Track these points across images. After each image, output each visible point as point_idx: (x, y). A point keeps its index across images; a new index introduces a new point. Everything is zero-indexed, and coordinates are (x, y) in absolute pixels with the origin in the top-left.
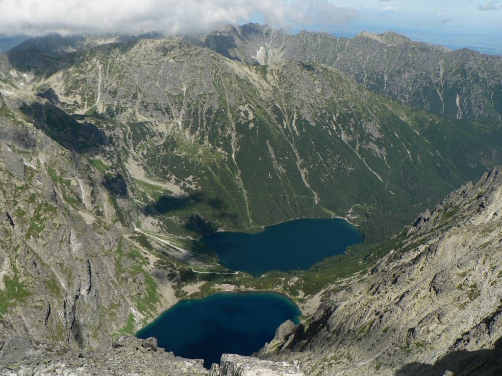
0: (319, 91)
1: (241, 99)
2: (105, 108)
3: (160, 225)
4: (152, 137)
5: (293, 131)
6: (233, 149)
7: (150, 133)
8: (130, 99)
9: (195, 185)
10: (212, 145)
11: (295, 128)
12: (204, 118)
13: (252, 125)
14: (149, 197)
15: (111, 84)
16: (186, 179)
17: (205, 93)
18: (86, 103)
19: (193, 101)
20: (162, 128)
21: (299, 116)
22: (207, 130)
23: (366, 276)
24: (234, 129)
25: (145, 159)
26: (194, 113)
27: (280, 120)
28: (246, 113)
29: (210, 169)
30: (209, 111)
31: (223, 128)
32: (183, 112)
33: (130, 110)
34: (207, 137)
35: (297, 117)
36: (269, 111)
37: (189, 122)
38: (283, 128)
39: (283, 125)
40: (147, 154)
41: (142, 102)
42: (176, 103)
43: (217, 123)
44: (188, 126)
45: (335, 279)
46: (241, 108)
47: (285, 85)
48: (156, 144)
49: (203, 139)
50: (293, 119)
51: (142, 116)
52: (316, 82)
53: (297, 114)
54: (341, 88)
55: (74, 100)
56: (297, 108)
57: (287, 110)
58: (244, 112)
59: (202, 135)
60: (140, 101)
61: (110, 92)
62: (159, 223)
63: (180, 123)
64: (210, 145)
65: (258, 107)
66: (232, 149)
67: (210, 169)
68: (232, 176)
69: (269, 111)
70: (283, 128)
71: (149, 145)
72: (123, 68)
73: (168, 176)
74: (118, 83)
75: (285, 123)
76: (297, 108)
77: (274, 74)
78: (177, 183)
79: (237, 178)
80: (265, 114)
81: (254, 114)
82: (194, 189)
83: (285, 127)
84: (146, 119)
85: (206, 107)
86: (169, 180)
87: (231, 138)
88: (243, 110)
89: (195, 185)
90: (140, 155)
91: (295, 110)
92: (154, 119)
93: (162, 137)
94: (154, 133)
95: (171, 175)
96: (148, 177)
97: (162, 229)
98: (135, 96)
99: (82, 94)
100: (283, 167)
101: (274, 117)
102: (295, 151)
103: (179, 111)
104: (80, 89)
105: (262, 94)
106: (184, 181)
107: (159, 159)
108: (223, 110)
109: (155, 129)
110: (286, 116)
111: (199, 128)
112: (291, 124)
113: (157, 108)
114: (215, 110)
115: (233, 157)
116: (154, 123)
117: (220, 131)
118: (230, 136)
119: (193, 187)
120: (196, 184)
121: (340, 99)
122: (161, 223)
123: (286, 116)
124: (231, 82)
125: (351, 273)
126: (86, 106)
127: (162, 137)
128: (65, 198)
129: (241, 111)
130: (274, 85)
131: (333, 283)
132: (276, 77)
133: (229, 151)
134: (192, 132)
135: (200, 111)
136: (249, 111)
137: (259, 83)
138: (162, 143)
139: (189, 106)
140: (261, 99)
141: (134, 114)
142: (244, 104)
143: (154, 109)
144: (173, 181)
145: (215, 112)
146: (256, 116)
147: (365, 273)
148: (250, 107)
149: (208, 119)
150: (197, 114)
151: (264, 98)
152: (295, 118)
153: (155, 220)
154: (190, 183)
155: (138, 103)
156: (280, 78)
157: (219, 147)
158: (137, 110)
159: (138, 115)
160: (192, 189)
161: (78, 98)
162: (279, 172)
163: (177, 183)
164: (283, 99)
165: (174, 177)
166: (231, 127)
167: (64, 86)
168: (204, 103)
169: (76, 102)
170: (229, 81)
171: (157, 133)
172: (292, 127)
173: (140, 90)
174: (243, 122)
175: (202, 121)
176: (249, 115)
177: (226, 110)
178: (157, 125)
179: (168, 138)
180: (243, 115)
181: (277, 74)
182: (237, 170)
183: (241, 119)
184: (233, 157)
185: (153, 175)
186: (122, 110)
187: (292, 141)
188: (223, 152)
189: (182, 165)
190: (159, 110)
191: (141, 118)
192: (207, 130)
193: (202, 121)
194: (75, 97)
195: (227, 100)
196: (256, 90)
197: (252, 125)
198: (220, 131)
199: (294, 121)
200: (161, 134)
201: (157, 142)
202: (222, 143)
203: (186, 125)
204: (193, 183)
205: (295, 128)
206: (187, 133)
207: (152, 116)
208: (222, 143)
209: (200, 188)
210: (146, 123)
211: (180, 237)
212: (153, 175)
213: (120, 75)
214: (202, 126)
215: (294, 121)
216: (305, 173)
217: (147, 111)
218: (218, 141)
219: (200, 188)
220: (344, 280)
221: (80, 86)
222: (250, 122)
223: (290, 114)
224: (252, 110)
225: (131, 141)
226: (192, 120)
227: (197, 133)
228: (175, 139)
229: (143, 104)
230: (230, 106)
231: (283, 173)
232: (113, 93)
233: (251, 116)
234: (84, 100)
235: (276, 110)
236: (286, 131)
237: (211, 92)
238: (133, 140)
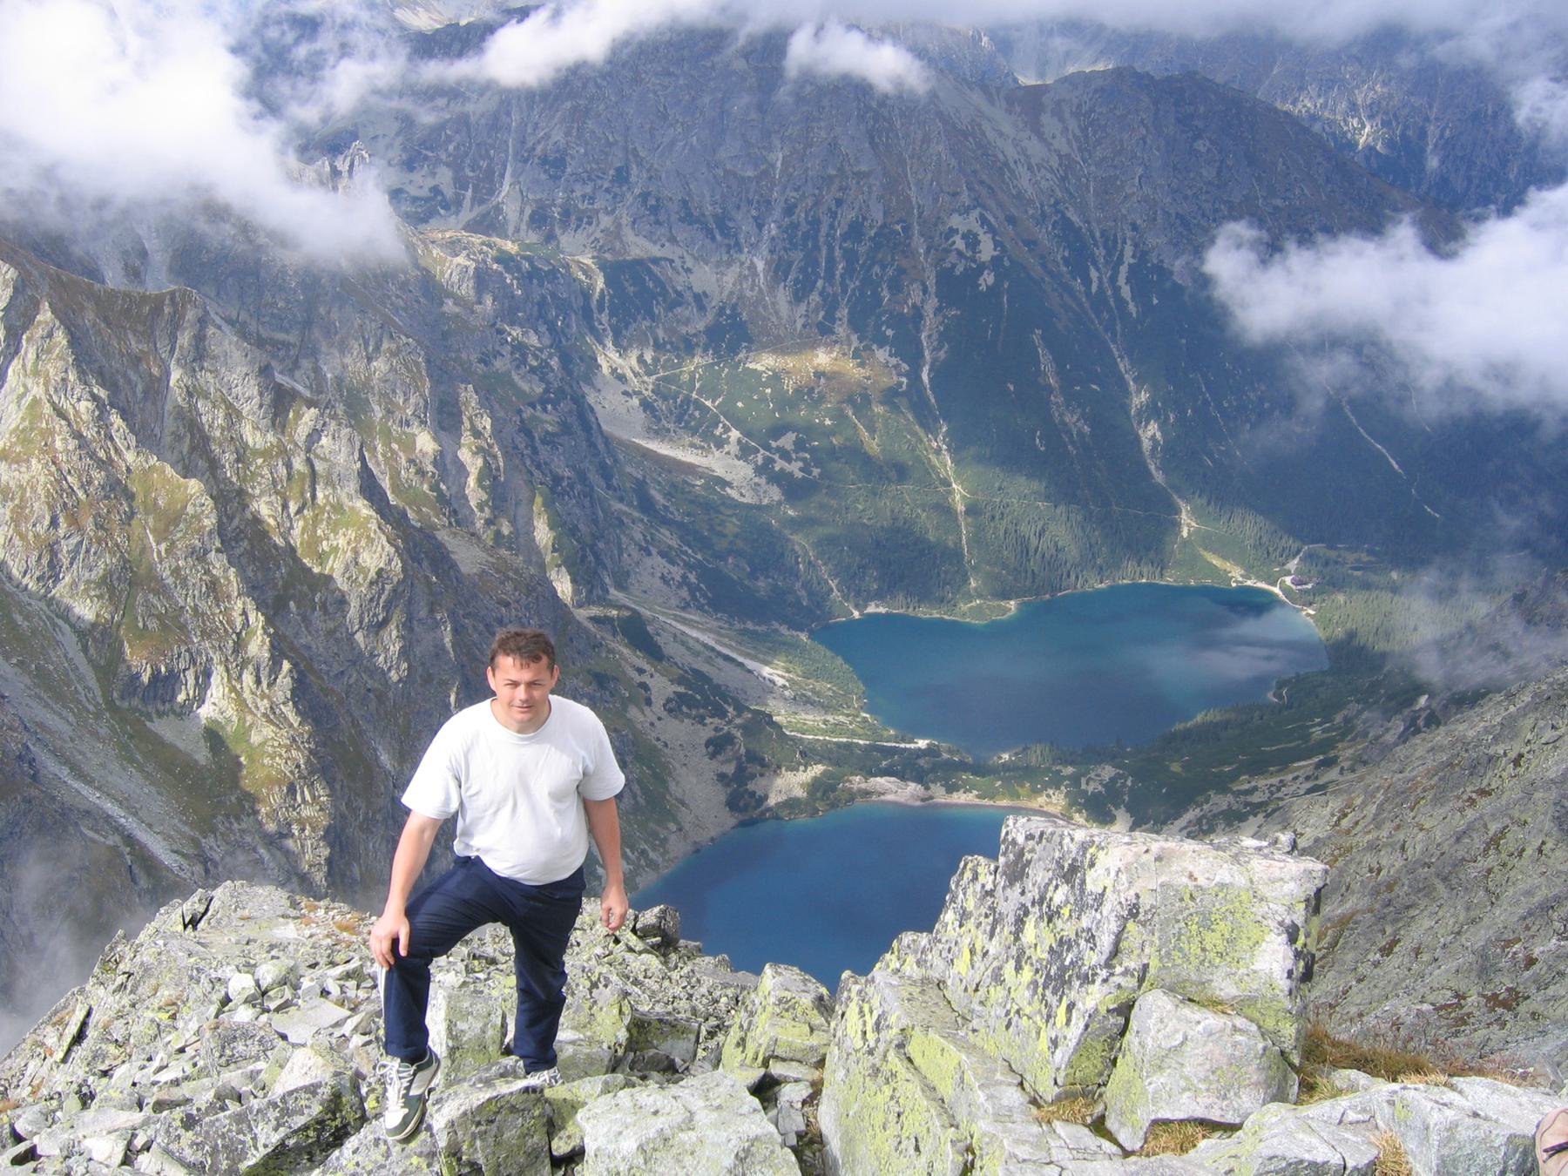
0: (1208, 173)
1: (955, 194)
2: (528, 211)
3: (689, 585)
4: (671, 307)
5: (1121, 302)
6: (927, 353)
7: (665, 293)
8: (606, 185)
9: (800, 464)
10: (860, 339)
11: (1126, 292)
12: (838, 253)
13: (987, 279)
14: (658, 497)
15: (547, 136)
16: (774, 444)
17: (841, 170)
18: (469, 193)
19: (803, 197)
20: (704, 278)
21: (1142, 255)
22: (844, 291)
23: (1333, 774)
24: (932, 289)
25: (649, 374)
26: (806, 236)
27: (1080, 260)
28: (972, 241)
30: (855, 231)
31: (896, 287)
32: (772, 229)
33: (606, 221)
34: (843, 313)
36: (1043, 235)
37: (790, 264)
38: (1088, 293)
39: (1087, 282)
40: (656, 360)
41: (645, 196)
42: (750, 202)
43: (877, 269)
44: (786, 276)
45: (1234, 777)
46: (956, 221)
47: (1098, 154)
48: (683, 330)
49: (830, 317)
50: (1120, 261)
51: (642, 241)
52: (1201, 146)
53: (1136, 246)
54: (1280, 166)
55: (430, 183)
56: (1135, 227)
57: (1103, 233)
58: (963, 237)
59: (830, 306)
60: (637, 191)
61: (544, 160)
62: (684, 577)
63: (760, 265)
64: (854, 337)
65: (1011, 220)
66: (921, 354)
68: (922, 441)
69: (1043, 235)
70: (1088, 293)
71: (661, 333)
72: (584, 86)
73: (717, 432)
74: (568, 134)
75: (1094, 274)
76: (1135, 227)
77: (1067, 115)
78: (745, 453)
80: (1031, 243)
81: (996, 244)
82: (799, 475)
84: (655, 251)
85: (848, 215)
86: (720, 443)
87: (921, 317)
88: (963, 229)
89: (800, 464)
90: (634, 361)
91: (1129, 234)
92: (679, 251)
93: (702, 308)
94: (679, 294)
95: (727, 430)
96: (657, 432)
97: (694, 598)
98: (622, 177)
99: (456, 166)
100: (1083, 415)
101: (1061, 253)
103: (760, 227)
104: (451, 148)
105: (1025, 182)
106: (768, 448)
107: (692, 379)
108: (898, 227)
109: (680, 281)
110: (1100, 252)
111: (820, 283)
112: (1113, 279)
113: (689, 216)
114: (871, 227)
115: (925, 377)
116: (678, 263)
117: (886, 294)
118: (918, 315)
119: (795, 468)
120: (804, 460)
121: (1279, 202)
122: (692, 578)
123: (1100, 252)
124: (926, 140)
125: (1284, 761)
126: (467, 203)
127: (702, 308)
128: (396, 488)
129: (957, 231)
130: (1065, 150)
131: (1223, 789)
132: (1073, 125)
133: (915, 360)
134: (799, 296)
135: (824, 229)
136: (980, 232)
137: (1016, 143)
138: (701, 326)
139: (789, 210)
140: (1019, 196)
141: (617, 233)
142: (966, 211)
143: (681, 220)
144: (733, 448)
145: (872, 233)
146: (1004, 250)
147: (1329, 763)
148: (983, 221)
149: (851, 257)
150: (816, 239)
151: (1030, 192)
152: (1128, 258)
153: (674, 569)
154: (785, 455)
155: (630, 198)
156: (1084, 130)
157: (881, 346)
158: (626, 220)
159: (629, 235)
160: (791, 474)
161: (445, 177)
162: (1069, 433)
163: (745, 453)
164: (1092, 200)
165: (735, 434)
166: (924, 284)
167: (400, 139)
168: (839, 202)
169: (436, 190)
170: (920, 136)
171: (688, 296)
172: (1116, 290)
173: (636, 155)
174: (960, 269)
175: (831, 261)
176: (981, 247)
177: (906, 229)
178: (688, 270)
179: (721, 310)
180: (960, 244)
181: (1076, 115)
182: (936, 420)
183: (953, 258)
184: (925, 377)
185: (671, 426)
186: (580, 220)
187: (1114, 335)
188: (893, 361)
189: (763, 399)
190: (697, 221)
191: (638, 247)
192: (844, 291)
193: (831, 261)
194: (434, 174)
195: (913, 193)
196: (1006, 164)
197: (987, 279)
198: (886, 294)
199: (1124, 270)
200: (700, 300)
201: (687, 322)
202: (890, 333)
203: (779, 270)
205: (1126, 292)
206: (783, 296)
207: (673, 240)
208: (890, 333)
209: (816, 471)
210: (656, 261)
211: (750, 626)
212: (671, 426)
213: (575, 109)
214: (830, 277)
215: (1124, 270)
216: (1153, 438)
217: (658, 223)
218: (878, 327)
219: (816, 471)
220: (1261, 782)
221: (449, 140)
222: (982, 268)
223: (1112, 246)
224: (992, 230)
225: (604, 317)
226: (797, 256)
227: (815, 297)
228: (745, 316)
229: (645, 202)
230: (920, 214)
231: (1080, 432)
232: (554, 164)
233: (987, 251)
234: (460, 183)
235: (1068, 233)
236: (1099, 301)
237: (864, 168)
238: (611, 315)
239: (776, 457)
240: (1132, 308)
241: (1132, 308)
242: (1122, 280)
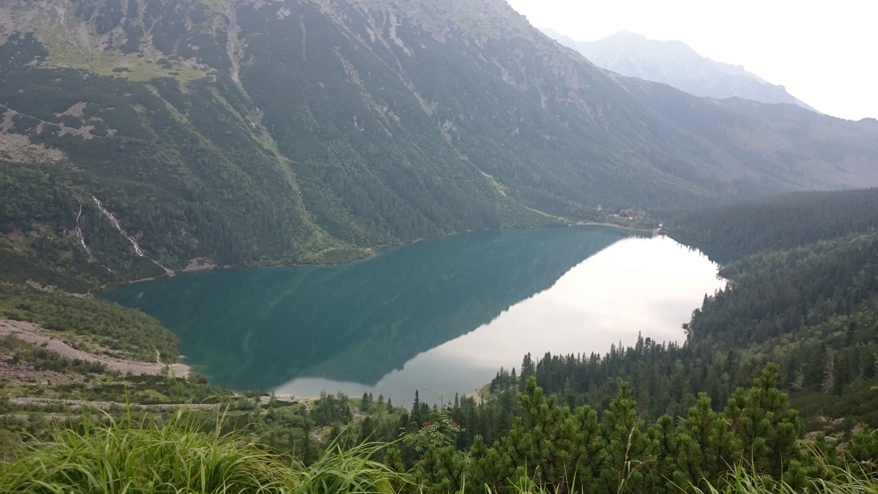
9: (91, 128)
11: (399, 42)
16: (59, 115)
29: (155, 92)
35: (398, 22)
39: (367, 37)
50: (389, 24)
57: (370, 10)
67: (155, 92)
75: (369, 31)
79: (254, 125)
83: (373, 39)
89: (91, 128)
112: (386, 35)
118: (223, 38)
119: (85, 132)
157: (187, 57)
160: (80, 137)
184: (235, 78)
202: (195, 48)
204: (84, 121)
205: (399, 42)
241: (406, 50)
242: (393, 35)
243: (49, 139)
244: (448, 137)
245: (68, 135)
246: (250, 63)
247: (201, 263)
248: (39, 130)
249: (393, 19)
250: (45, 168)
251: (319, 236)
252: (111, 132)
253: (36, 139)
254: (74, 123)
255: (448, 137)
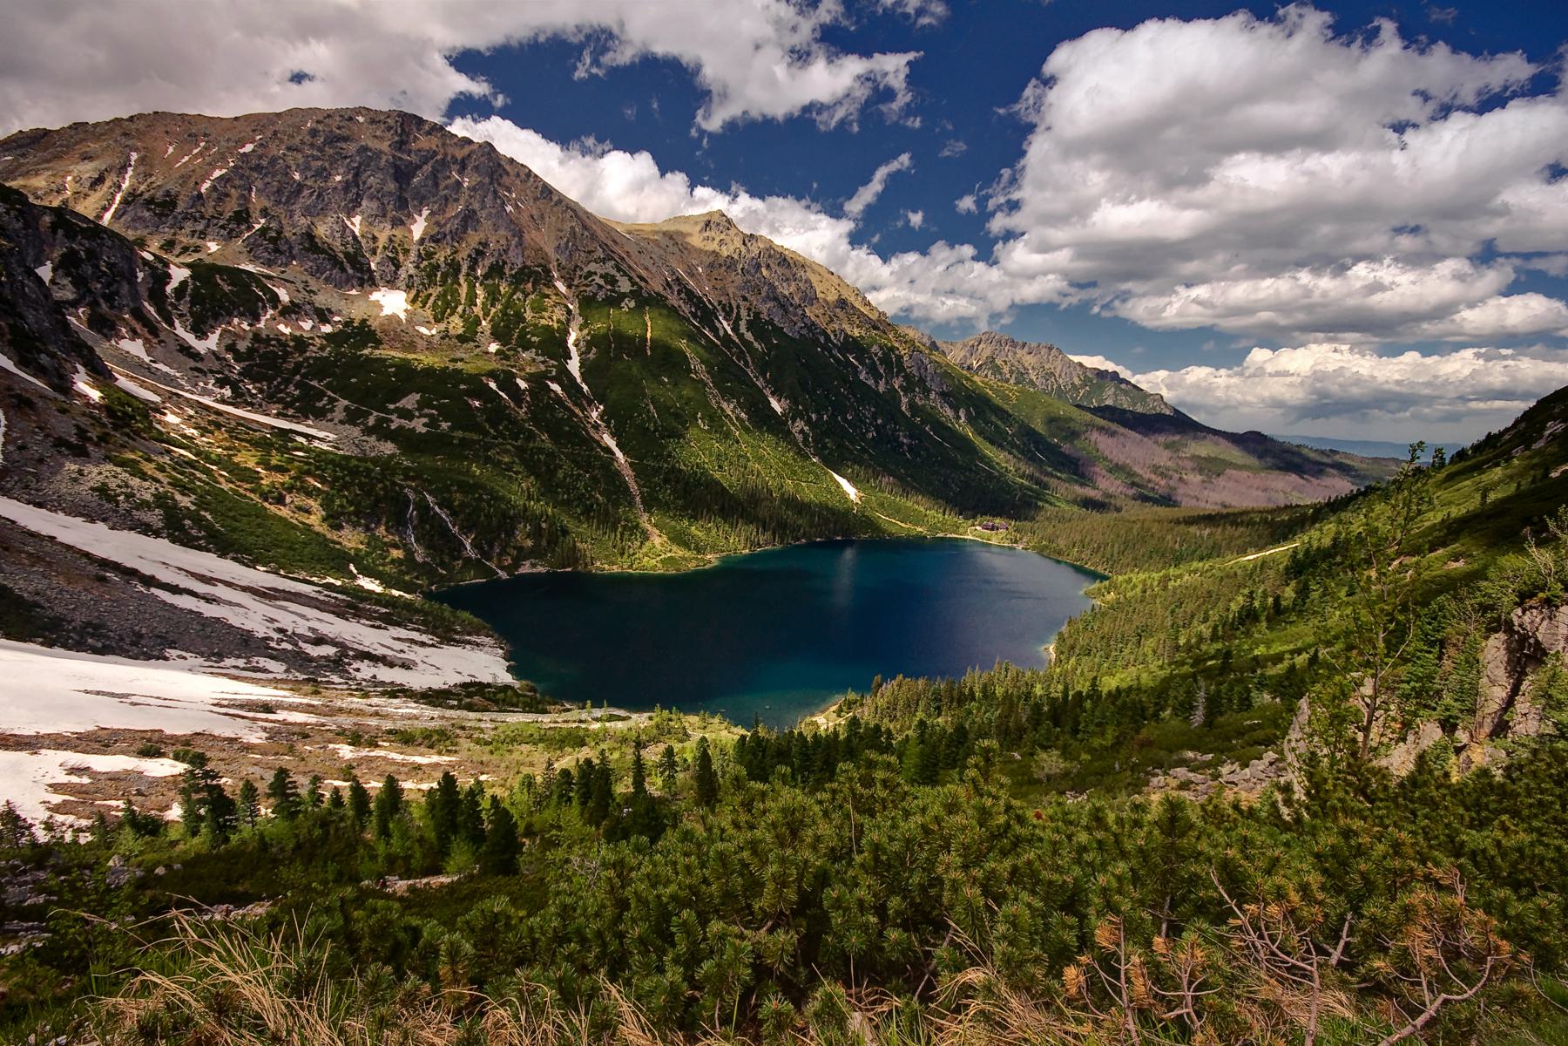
9: (425, 420)
11: (749, 336)
16: (392, 407)
50: (739, 318)
89: (425, 420)
102: (760, 383)
119: (419, 425)
120: (430, 416)
143: (307, 250)
157: (525, 349)
172: (741, 336)
205: (749, 336)
238: (193, 303)
239: (394, 417)
240: (756, 345)
241: (756, 345)
242: (743, 329)
243: (382, 431)
244: (800, 438)
245: (401, 428)
246: (591, 356)
247: (534, 566)
248: (371, 421)
249: (744, 313)
250: (375, 461)
251: (657, 541)
252: (445, 425)
253: (368, 431)
254: (406, 414)
255: (800, 438)
